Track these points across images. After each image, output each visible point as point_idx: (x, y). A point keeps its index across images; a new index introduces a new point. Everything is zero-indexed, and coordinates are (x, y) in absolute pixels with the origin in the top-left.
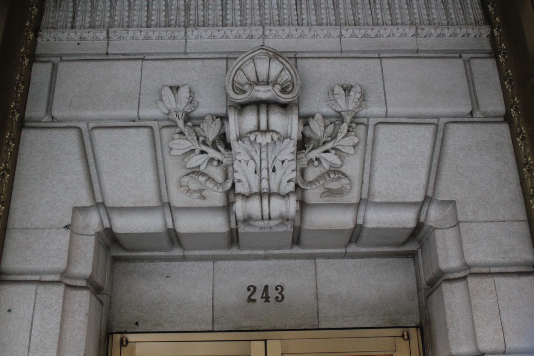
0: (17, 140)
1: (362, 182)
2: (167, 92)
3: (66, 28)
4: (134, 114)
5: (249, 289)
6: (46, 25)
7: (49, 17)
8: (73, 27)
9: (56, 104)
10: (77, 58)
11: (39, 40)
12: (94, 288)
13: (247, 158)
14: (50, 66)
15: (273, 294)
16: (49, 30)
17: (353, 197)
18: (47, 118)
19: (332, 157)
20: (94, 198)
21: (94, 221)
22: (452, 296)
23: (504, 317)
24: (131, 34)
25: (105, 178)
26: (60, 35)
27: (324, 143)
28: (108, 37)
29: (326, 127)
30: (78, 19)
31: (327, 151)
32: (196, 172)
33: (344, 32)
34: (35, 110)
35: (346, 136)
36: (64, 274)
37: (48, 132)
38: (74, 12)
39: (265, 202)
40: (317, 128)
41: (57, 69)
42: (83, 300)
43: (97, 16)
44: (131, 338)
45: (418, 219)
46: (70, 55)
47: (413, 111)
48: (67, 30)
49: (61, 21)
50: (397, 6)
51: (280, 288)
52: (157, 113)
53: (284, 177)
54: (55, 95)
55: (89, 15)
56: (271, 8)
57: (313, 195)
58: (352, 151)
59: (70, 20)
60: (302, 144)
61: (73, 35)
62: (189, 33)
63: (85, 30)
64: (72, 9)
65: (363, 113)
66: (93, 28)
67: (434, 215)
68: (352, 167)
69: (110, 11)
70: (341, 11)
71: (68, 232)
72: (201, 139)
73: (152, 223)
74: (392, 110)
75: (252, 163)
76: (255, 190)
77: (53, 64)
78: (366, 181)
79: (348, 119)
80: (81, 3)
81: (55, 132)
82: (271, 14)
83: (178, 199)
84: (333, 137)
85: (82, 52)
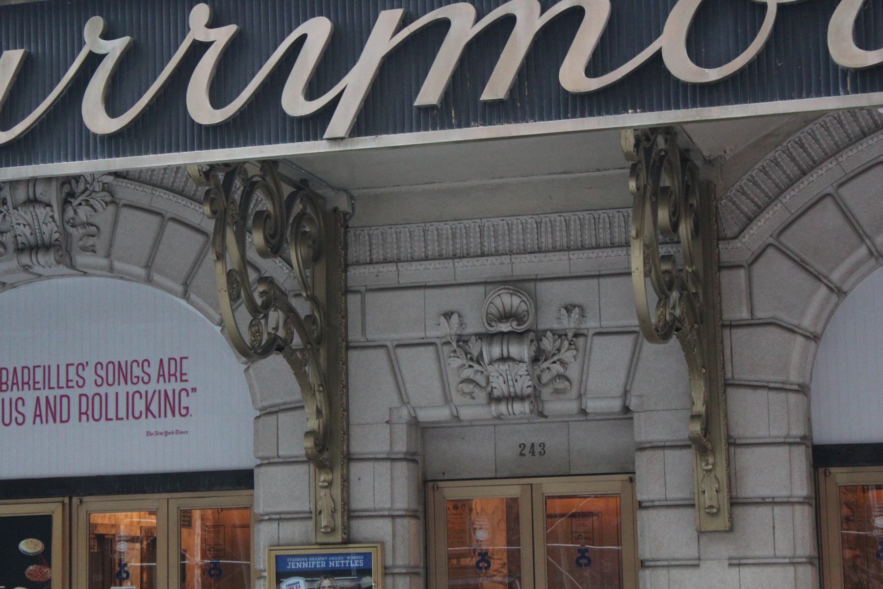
0: (346, 363)
1: (582, 381)
2: (443, 320)
4: (422, 335)
5: (520, 446)
9: (367, 331)
12: (411, 458)
13: (497, 375)
15: (537, 449)
17: (574, 393)
19: (557, 368)
20: (403, 401)
21: (404, 413)
22: (642, 461)
23: (668, 478)
24: (414, 267)
25: (407, 385)
26: (363, 270)
27: (554, 355)
28: (398, 270)
29: (555, 341)
31: (554, 362)
32: (468, 381)
33: (571, 256)
34: (355, 335)
35: (568, 349)
36: (390, 453)
38: (371, 245)
39: (510, 406)
40: (548, 344)
42: (402, 468)
44: (441, 484)
45: (625, 403)
47: (620, 323)
50: (616, 224)
51: (542, 445)
52: (438, 334)
53: (524, 385)
56: (517, 233)
57: (546, 393)
58: (573, 360)
59: (368, 254)
60: (535, 360)
62: (456, 265)
64: (368, 243)
65: (583, 326)
67: (633, 403)
68: (573, 372)
70: (572, 233)
71: (388, 426)
72: (469, 356)
73: (442, 414)
74: (604, 323)
75: (501, 377)
76: (506, 393)
78: (584, 380)
79: (570, 335)
82: (518, 239)
83: (457, 398)
84: (559, 350)
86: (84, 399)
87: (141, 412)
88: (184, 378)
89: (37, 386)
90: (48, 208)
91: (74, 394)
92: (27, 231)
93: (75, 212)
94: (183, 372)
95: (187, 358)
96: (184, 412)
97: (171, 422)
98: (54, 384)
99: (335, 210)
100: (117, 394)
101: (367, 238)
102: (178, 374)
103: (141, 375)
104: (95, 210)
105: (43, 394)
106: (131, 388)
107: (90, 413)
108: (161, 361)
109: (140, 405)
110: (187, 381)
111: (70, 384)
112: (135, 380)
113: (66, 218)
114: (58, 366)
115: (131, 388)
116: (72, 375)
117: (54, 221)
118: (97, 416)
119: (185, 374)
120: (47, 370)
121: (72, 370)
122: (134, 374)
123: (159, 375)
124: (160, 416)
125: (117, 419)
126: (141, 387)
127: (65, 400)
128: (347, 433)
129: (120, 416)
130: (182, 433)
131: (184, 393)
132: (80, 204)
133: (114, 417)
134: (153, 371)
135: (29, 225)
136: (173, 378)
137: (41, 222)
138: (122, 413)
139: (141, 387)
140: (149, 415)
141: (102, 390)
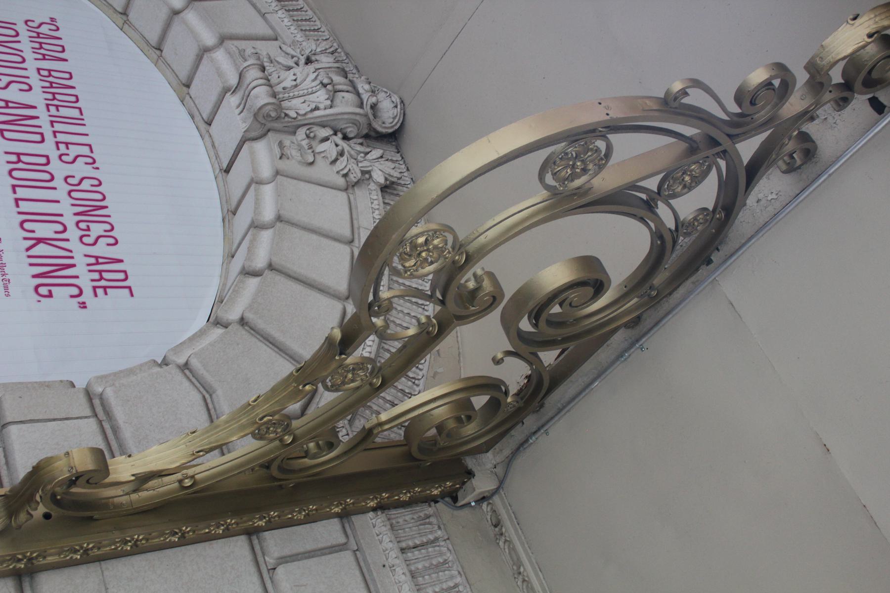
0: (228, 534)
3: (398, 542)
6: (393, 516)
7: (403, 516)
8: (403, 550)
10: (365, 570)
11: (371, 514)
14: (342, 540)
16: (388, 523)
18: (271, 561)
26: (386, 539)
30: (416, 553)
34: (276, 543)
37: (252, 569)
41: (341, 551)
43: (429, 575)
46: (365, 560)
48: (396, 544)
49: (405, 532)
54: (305, 561)
55: (427, 565)
59: (411, 543)
61: (393, 554)
63: (405, 567)
64: (425, 540)
66: (413, 577)
69: (443, 589)
77: (345, 544)
80: (437, 548)
81: (255, 579)
85: (375, 574)
86: (43, 160)
87: (33, 231)
88: (100, 292)
89: (52, 109)
90: (329, 102)
91: (49, 148)
92: (288, 83)
93: (326, 139)
94: (108, 290)
95: (132, 295)
96: (43, 290)
97: (21, 272)
98: (58, 127)
99: (470, 474)
100: (58, 202)
101: (431, 537)
102: (103, 283)
103: (94, 234)
104: (334, 162)
105: (41, 111)
106: (70, 220)
107: (20, 165)
108: (121, 261)
109: (44, 230)
110: (96, 295)
111: (62, 146)
112: (83, 225)
113: (315, 128)
114: (87, 135)
115: (70, 220)
116: (74, 151)
117: (312, 110)
118: (15, 174)
119: (106, 293)
120: (79, 121)
121: (85, 150)
122: (92, 225)
123: (97, 258)
124: (29, 257)
125: (17, 200)
126: (73, 233)
127: (38, 138)
128: (88, 559)
129: (20, 203)
130: (6, 288)
131: (75, 291)
132: (337, 145)
133: (18, 196)
134: (101, 249)
135: (296, 86)
136: (96, 276)
137: (306, 98)
138: (25, 206)
139: (73, 233)
140: (33, 242)
141: (58, 182)
